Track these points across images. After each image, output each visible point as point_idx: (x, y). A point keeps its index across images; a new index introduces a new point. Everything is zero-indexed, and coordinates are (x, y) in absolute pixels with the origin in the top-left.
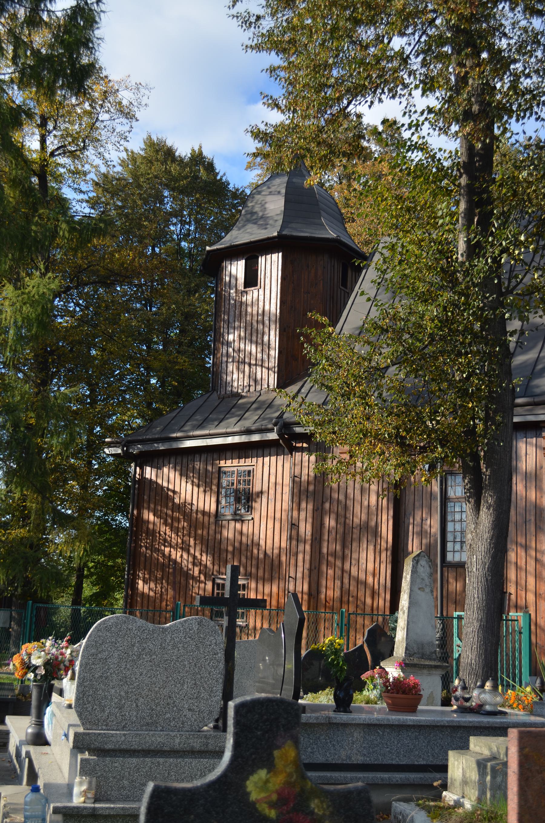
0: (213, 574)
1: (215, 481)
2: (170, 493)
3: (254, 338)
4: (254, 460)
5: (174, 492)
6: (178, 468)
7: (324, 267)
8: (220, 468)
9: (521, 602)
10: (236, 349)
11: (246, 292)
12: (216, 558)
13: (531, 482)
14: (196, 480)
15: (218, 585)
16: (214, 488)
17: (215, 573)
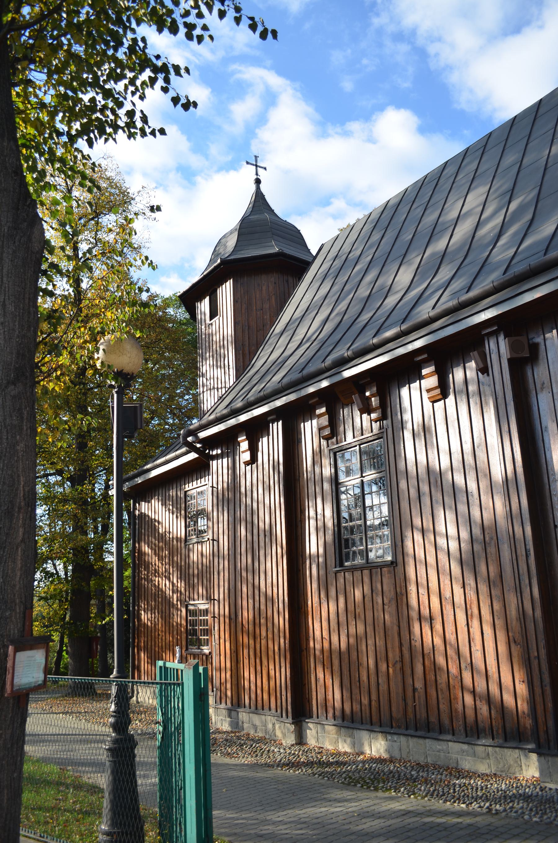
0: (186, 601)
1: (183, 506)
2: (157, 524)
3: (219, 364)
4: (203, 480)
5: (159, 522)
6: (160, 498)
7: (275, 283)
8: (186, 492)
9: (425, 612)
10: (208, 378)
11: (212, 324)
12: (187, 584)
13: (420, 439)
14: (171, 507)
15: (190, 611)
16: (183, 512)
17: (187, 599)
